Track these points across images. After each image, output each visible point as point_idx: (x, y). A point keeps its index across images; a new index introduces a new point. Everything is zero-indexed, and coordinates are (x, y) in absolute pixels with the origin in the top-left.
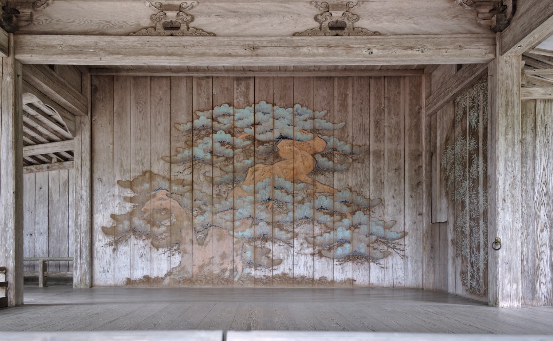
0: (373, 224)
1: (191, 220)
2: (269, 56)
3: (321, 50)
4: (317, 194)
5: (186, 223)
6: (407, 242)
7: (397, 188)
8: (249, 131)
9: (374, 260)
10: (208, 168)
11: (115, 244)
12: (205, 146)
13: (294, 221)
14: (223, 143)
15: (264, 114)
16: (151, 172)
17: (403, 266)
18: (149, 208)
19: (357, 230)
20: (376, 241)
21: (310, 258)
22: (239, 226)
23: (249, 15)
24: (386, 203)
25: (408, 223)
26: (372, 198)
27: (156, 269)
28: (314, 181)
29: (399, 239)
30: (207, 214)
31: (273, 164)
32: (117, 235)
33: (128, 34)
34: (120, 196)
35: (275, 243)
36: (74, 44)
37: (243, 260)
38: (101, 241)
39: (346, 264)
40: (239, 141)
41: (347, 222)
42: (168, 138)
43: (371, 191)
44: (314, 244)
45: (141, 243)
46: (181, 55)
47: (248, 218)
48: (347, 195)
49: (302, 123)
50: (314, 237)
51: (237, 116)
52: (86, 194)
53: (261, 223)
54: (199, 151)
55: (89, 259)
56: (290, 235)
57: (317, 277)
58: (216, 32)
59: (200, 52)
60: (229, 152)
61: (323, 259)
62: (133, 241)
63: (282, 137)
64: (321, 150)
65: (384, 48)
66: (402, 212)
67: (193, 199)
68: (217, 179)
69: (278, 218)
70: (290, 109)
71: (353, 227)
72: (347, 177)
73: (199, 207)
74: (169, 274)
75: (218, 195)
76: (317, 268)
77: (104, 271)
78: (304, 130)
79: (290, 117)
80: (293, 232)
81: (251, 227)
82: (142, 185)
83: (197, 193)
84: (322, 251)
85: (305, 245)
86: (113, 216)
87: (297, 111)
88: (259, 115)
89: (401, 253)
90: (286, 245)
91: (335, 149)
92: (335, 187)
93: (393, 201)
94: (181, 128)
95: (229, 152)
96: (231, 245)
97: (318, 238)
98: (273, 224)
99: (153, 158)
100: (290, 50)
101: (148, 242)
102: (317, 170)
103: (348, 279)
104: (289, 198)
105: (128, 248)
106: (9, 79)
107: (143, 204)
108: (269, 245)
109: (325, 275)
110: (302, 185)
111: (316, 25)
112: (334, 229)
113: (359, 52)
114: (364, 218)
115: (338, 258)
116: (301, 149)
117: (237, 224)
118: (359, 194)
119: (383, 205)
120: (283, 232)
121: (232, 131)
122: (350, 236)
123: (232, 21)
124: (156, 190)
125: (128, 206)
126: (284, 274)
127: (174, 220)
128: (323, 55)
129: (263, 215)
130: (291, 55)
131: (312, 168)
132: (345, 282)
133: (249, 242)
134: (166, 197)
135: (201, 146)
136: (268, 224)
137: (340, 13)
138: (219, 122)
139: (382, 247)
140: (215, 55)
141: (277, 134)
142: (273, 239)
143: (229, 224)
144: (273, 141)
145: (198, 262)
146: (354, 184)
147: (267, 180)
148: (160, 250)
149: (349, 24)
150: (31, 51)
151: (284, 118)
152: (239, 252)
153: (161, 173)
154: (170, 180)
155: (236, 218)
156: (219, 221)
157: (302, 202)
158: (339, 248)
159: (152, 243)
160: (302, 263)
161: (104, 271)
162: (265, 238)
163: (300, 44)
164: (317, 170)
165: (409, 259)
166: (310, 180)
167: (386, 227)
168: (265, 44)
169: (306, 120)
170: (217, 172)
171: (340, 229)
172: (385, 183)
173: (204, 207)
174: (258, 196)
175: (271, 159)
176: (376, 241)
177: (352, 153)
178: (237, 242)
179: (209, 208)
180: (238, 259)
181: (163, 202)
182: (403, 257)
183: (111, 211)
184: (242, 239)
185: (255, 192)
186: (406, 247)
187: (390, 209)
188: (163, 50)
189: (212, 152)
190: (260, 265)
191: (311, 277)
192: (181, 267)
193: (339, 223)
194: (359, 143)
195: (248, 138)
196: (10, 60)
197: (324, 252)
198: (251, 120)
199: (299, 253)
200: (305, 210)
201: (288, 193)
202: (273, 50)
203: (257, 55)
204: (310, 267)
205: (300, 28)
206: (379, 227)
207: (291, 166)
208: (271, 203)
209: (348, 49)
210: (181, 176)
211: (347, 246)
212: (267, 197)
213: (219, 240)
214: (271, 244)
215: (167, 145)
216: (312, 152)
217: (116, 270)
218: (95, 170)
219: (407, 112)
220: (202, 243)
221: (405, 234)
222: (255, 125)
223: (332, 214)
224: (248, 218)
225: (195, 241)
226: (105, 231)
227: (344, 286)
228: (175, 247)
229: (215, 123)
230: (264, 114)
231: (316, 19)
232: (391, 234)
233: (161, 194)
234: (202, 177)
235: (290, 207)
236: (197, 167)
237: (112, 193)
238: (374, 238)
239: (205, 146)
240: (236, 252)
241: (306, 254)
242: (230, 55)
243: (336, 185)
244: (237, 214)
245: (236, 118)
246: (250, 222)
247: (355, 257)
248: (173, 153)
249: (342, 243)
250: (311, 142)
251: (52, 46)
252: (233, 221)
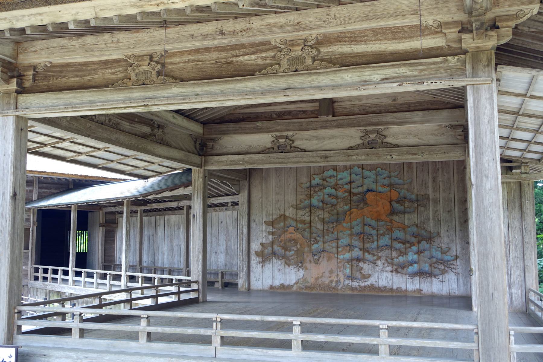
0: (434, 250)
1: (310, 246)
2: (334, 161)
3: (363, 157)
4: (393, 229)
5: (306, 249)
6: (458, 263)
7: (450, 224)
8: (347, 187)
9: (435, 276)
10: (321, 212)
11: (263, 262)
12: (318, 198)
13: (378, 248)
14: (330, 195)
15: (357, 175)
16: (285, 215)
17: (456, 281)
18: (283, 239)
19: (422, 254)
20: (436, 262)
21: (390, 274)
22: (342, 251)
23: (324, 138)
24: (442, 235)
25: (459, 249)
26: (432, 232)
27: (288, 280)
28: (391, 220)
29: (452, 260)
30: (320, 243)
31: (363, 209)
32: (265, 257)
33: (259, 153)
34: (266, 231)
35: (365, 263)
36: (233, 159)
37: (344, 275)
38: (255, 260)
39: (415, 278)
40: (340, 194)
41: (415, 248)
42: (295, 192)
43: (431, 227)
44: (392, 264)
45: (278, 262)
46: (286, 163)
47: (347, 246)
48: (415, 229)
49: (382, 180)
50: (392, 259)
51: (339, 177)
52: (245, 230)
53: (356, 249)
54: (315, 201)
55: (247, 272)
56: (375, 258)
57: (395, 287)
58: (306, 149)
59: (297, 161)
60: (334, 201)
61: (399, 275)
62: (274, 260)
63: (369, 191)
64: (395, 199)
65: (400, 155)
66: (454, 242)
67: (311, 233)
68: (327, 219)
69: (367, 245)
70: (374, 171)
71: (420, 252)
72: (414, 217)
73: (315, 238)
74: (296, 283)
75: (327, 230)
76: (394, 281)
77: (256, 280)
78: (383, 186)
79: (374, 177)
80: (378, 255)
81: (349, 252)
82: (279, 224)
83: (313, 228)
84: (398, 269)
85: (386, 265)
86: (262, 244)
87: (378, 172)
88: (354, 176)
89: (455, 271)
90: (373, 265)
91: (405, 198)
92: (406, 224)
93: (447, 233)
94: (303, 186)
95: (334, 201)
96: (336, 264)
97: (395, 260)
98: (364, 250)
99: (286, 206)
100: (346, 158)
101: (283, 261)
102: (393, 212)
103: (417, 289)
104: (374, 232)
105: (271, 265)
106: (201, 180)
107: (280, 236)
108: (361, 264)
109: (401, 286)
110: (383, 223)
111: (361, 142)
112: (406, 254)
113: (385, 157)
114: (427, 246)
115: (410, 274)
116: (381, 198)
117: (340, 249)
118: (422, 229)
119: (440, 236)
120: (371, 255)
121: (336, 187)
122: (417, 259)
123: (315, 142)
124: (288, 227)
125: (271, 237)
126: (372, 285)
127: (299, 247)
128: (365, 160)
129: (357, 243)
130: (346, 161)
131: (389, 211)
132: (415, 291)
133: (348, 262)
134: (293, 231)
135: (316, 197)
136: (361, 249)
137: (374, 135)
138: (327, 182)
139: (441, 267)
140: (305, 162)
141: (365, 188)
142: (364, 260)
143: (334, 249)
144: (363, 193)
145: (315, 275)
146: (419, 222)
147: (359, 220)
148: (291, 267)
149: (380, 141)
150: (212, 165)
151: (370, 177)
152: (342, 269)
153: (291, 216)
154: (296, 220)
155: (339, 246)
156: (328, 247)
157: (383, 235)
158: (410, 267)
159: (285, 262)
160: (384, 277)
161: (256, 280)
162: (358, 260)
163: (351, 154)
165: (461, 275)
166: (388, 219)
167: (444, 252)
168: (332, 155)
169: (384, 179)
170: (326, 215)
171: (410, 253)
172: (441, 220)
173: (318, 238)
174: (353, 230)
175: (362, 205)
176: (436, 262)
177: (417, 200)
178: (340, 262)
179: (321, 239)
180: (340, 274)
181: (293, 235)
182: (457, 274)
183: (260, 241)
184: (343, 260)
185: (351, 228)
186: (458, 267)
187: (445, 239)
188: (277, 160)
189: (323, 202)
190: (355, 278)
191: (391, 287)
192: (304, 279)
193: (409, 249)
194: (422, 193)
195: (346, 192)
196: (202, 170)
197: (399, 270)
198: (348, 179)
199: (382, 270)
200: (385, 240)
201: (373, 229)
202: (336, 158)
203: (328, 161)
204: (390, 280)
205: (352, 144)
206: (438, 252)
207: (376, 210)
208: (362, 235)
209: (379, 156)
210: (303, 218)
211: (416, 266)
212: (359, 231)
213: (328, 261)
214: (363, 263)
215: (295, 198)
216: (389, 200)
217: (264, 279)
218: (251, 214)
219: (455, 171)
220: (317, 262)
221: (457, 257)
222: (350, 182)
224: (347, 246)
225: (312, 261)
226: (257, 254)
227: (414, 294)
228: (300, 265)
229: (325, 182)
230: (357, 175)
231: (361, 139)
232: (446, 258)
233: (291, 229)
234: (316, 218)
235: (375, 238)
236: (313, 211)
237: (261, 229)
238: (434, 260)
239: (318, 198)
240: (340, 269)
241: (387, 271)
242: (313, 162)
243: (407, 222)
244: (340, 243)
245: (338, 178)
246: (348, 248)
247: (421, 274)
248: (298, 203)
249: (411, 263)
250: (389, 193)
251: (222, 162)
252: (337, 247)
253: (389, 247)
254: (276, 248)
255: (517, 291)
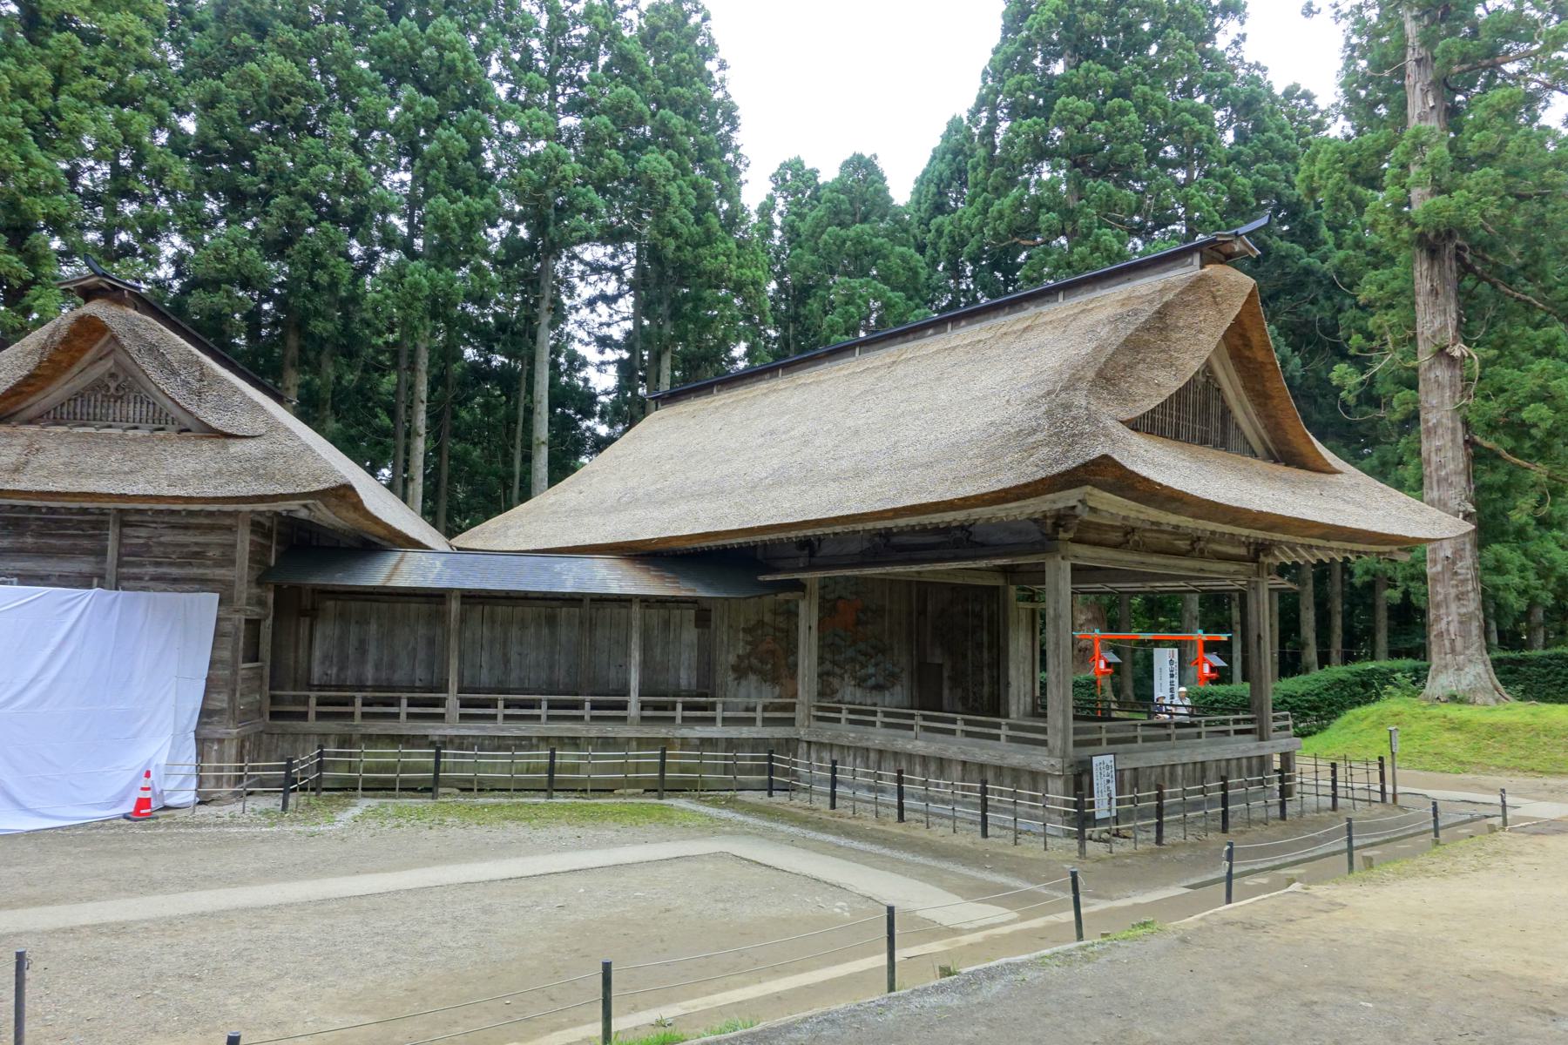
11: (738, 679)
44: (855, 678)
63: (840, 598)
71: (876, 665)
84: (860, 682)
98: (834, 663)
102: (858, 622)
162: (828, 674)
164: (858, 622)
200: (850, 653)
223: (865, 654)
232: (897, 670)
233: (769, 639)
253: (853, 660)
254: (754, 661)
255: (1029, 699)
